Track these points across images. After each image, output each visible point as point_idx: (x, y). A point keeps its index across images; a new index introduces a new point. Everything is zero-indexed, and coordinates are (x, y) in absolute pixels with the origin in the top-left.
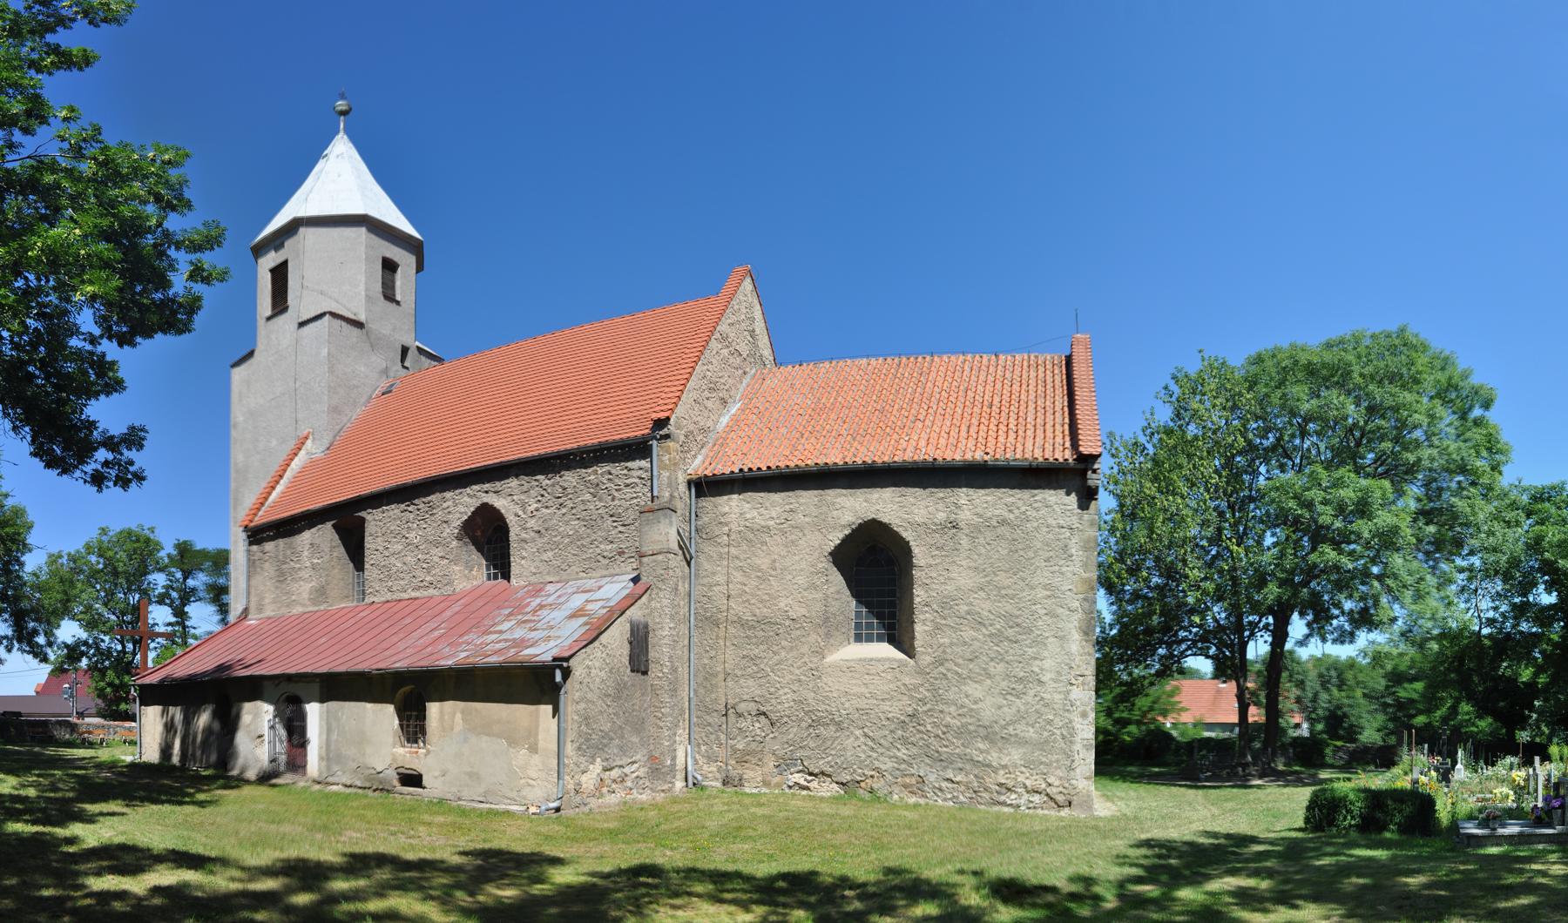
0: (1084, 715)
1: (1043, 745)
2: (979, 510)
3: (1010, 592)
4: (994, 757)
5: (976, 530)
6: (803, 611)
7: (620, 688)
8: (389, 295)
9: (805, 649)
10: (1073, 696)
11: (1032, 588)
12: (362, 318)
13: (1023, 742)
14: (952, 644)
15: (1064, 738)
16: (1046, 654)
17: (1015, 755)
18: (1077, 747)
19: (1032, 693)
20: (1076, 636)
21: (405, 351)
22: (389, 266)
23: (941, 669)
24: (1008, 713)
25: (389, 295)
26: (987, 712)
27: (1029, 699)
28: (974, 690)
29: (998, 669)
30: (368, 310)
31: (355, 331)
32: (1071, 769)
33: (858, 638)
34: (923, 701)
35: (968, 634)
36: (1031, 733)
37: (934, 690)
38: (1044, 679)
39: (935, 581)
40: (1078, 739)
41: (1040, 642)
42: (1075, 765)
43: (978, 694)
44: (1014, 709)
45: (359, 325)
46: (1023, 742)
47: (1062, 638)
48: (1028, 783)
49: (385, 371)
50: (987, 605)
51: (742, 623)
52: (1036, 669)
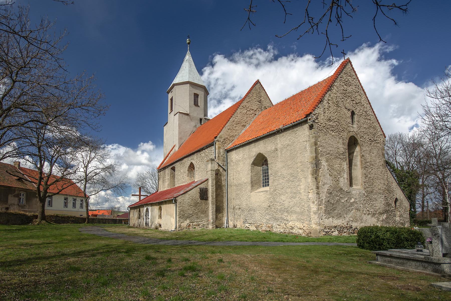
0: (313, 203)
1: (302, 213)
2: (282, 143)
3: (291, 166)
4: (289, 218)
5: (282, 149)
6: (247, 181)
7: (196, 204)
8: (196, 104)
9: (247, 191)
10: (310, 196)
11: (297, 164)
12: (188, 113)
13: (296, 213)
14: (277, 185)
15: (308, 210)
16: (301, 184)
17: (294, 217)
18: (312, 213)
19: (298, 197)
20: (310, 176)
21: (201, 120)
22: (196, 96)
23: (275, 192)
24: (292, 203)
25: (196, 104)
26: (286, 204)
27: (297, 199)
28: (283, 197)
29: (289, 190)
30: (190, 110)
31: (186, 117)
32: (310, 221)
33: (263, 186)
34: (271, 202)
35: (281, 181)
36: (298, 210)
37: (274, 199)
38: (301, 192)
39: (275, 166)
40: (312, 211)
41: (300, 180)
42: (311, 219)
43: (284, 199)
44: (293, 202)
45: (187, 115)
46: (296, 213)
47: (306, 178)
48: (298, 226)
49: (196, 126)
50: (285, 172)
51: (236, 185)
52: (299, 189)
